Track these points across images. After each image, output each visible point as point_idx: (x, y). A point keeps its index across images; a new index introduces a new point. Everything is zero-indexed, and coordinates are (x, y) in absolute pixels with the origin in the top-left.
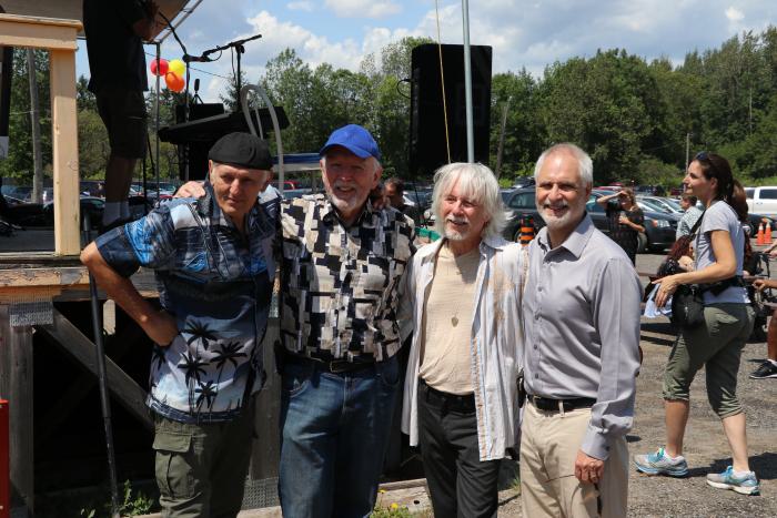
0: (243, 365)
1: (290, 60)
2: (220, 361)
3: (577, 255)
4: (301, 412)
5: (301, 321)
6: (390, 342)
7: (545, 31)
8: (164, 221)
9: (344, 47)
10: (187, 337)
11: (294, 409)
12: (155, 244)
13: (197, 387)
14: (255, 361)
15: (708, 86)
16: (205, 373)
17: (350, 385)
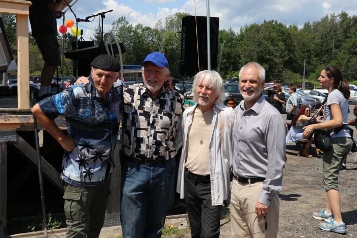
0: (105, 161)
2: (95, 159)
3: (257, 112)
4: (131, 182)
5: (132, 141)
6: (172, 151)
7: (240, 12)
8: (70, 94)
9: (148, 17)
10: (80, 147)
11: (128, 181)
12: (66, 105)
13: (84, 170)
14: (111, 159)
15: (314, 38)
16: (88, 164)
17: (154, 170)
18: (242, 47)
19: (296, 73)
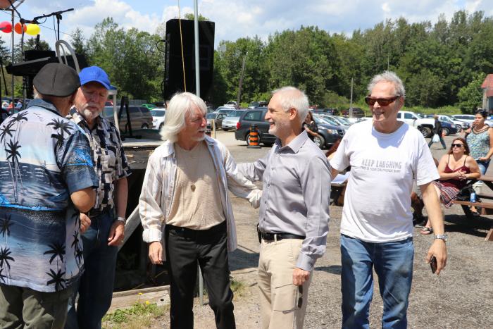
1: (110, 25)
15: (365, 50)
18: (271, 60)
19: (342, 95)
